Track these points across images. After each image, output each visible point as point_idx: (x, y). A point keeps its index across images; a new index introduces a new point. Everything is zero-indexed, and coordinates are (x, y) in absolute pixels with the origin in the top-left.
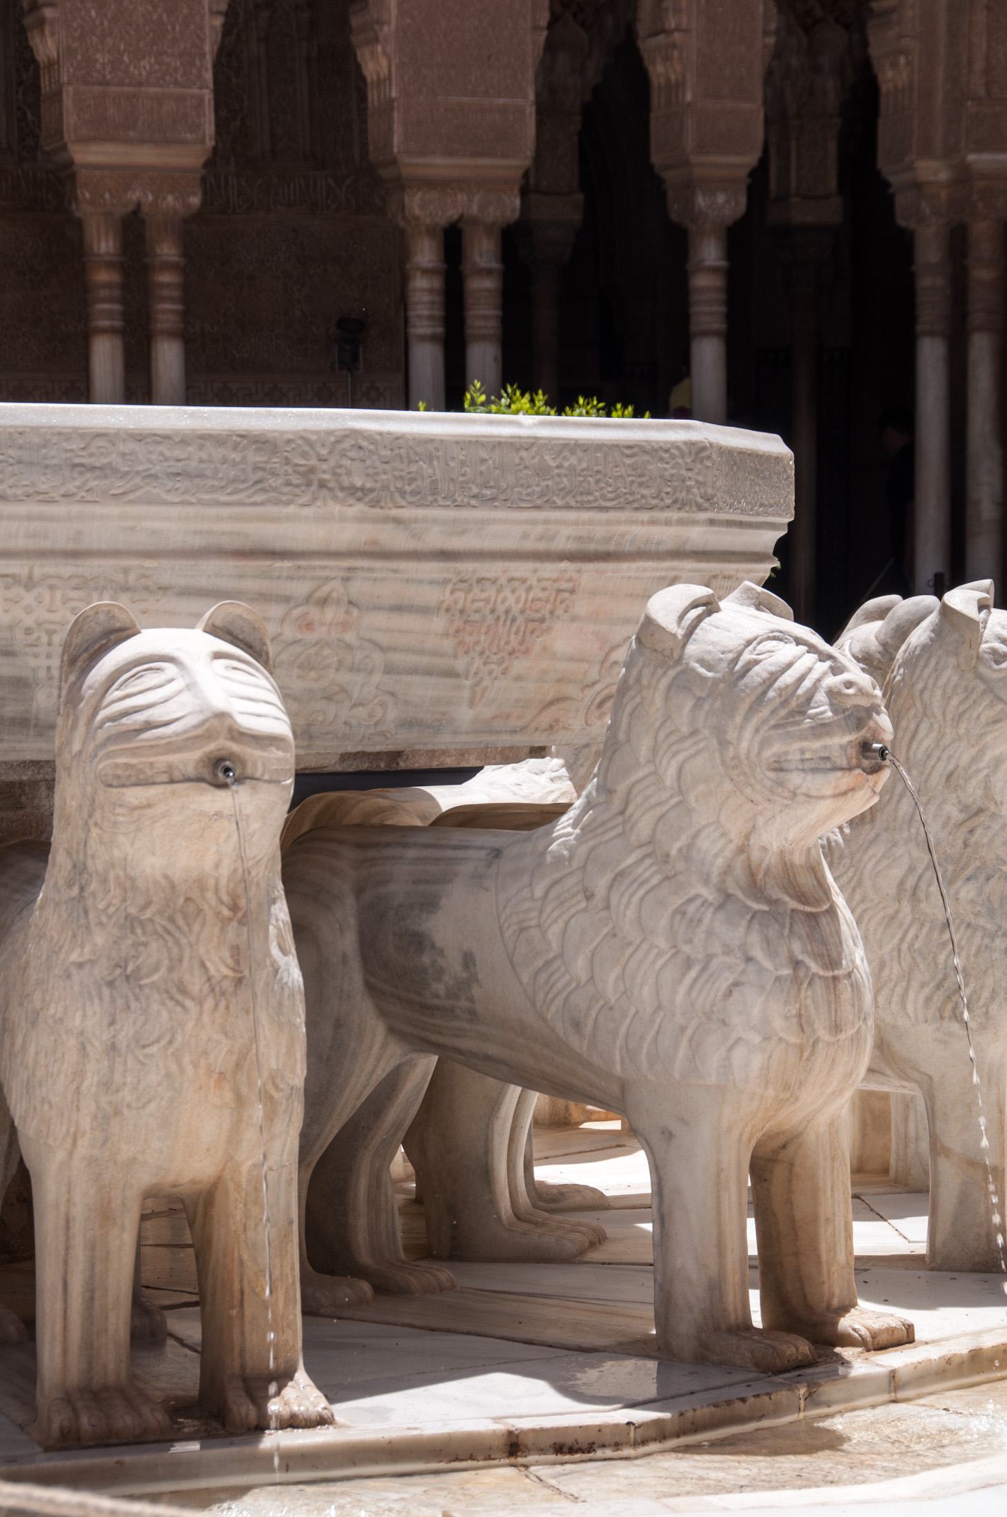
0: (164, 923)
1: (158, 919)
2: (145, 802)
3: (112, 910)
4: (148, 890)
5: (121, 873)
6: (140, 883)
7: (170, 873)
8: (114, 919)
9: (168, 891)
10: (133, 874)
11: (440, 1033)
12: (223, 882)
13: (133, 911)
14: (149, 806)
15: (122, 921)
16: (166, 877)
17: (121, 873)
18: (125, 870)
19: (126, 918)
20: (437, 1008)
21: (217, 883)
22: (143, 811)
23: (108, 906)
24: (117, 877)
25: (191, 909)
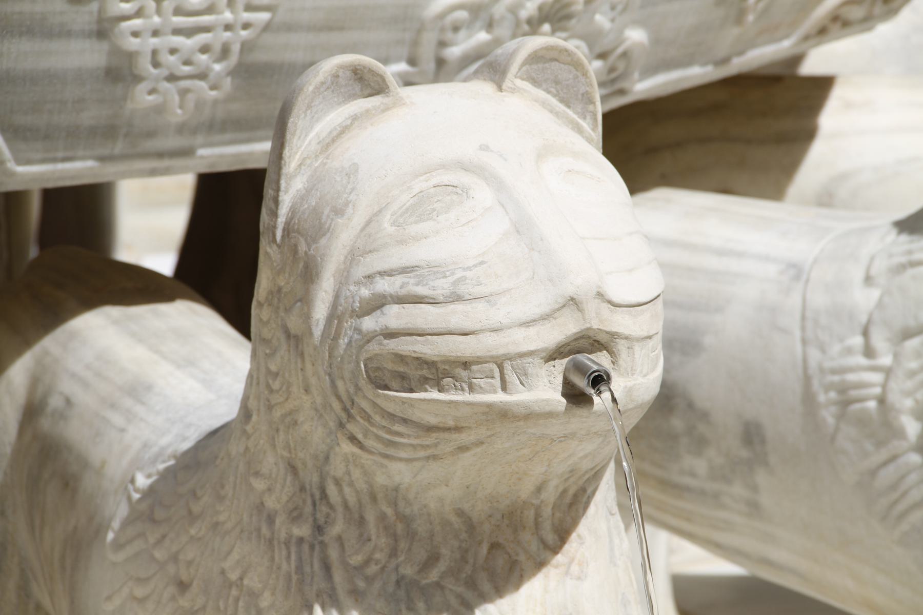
0: (460, 589)
1: (449, 583)
2: (451, 423)
4: (432, 536)
5: (389, 511)
6: (421, 527)
7: (466, 507)
8: (377, 585)
9: (464, 536)
10: (408, 511)
11: (688, 520)
12: (547, 511)
13: (408, 571)
14: (457, 429)
15: (391, 588)
16: (460, 513)
17: (389, 511)
18: (396, 505)
19: (398, 583)
20: (688, 489)
21: (538, 515)
22: (446, 435)
23: (367, 562)
24: (382, 517)
25: (500, 561)
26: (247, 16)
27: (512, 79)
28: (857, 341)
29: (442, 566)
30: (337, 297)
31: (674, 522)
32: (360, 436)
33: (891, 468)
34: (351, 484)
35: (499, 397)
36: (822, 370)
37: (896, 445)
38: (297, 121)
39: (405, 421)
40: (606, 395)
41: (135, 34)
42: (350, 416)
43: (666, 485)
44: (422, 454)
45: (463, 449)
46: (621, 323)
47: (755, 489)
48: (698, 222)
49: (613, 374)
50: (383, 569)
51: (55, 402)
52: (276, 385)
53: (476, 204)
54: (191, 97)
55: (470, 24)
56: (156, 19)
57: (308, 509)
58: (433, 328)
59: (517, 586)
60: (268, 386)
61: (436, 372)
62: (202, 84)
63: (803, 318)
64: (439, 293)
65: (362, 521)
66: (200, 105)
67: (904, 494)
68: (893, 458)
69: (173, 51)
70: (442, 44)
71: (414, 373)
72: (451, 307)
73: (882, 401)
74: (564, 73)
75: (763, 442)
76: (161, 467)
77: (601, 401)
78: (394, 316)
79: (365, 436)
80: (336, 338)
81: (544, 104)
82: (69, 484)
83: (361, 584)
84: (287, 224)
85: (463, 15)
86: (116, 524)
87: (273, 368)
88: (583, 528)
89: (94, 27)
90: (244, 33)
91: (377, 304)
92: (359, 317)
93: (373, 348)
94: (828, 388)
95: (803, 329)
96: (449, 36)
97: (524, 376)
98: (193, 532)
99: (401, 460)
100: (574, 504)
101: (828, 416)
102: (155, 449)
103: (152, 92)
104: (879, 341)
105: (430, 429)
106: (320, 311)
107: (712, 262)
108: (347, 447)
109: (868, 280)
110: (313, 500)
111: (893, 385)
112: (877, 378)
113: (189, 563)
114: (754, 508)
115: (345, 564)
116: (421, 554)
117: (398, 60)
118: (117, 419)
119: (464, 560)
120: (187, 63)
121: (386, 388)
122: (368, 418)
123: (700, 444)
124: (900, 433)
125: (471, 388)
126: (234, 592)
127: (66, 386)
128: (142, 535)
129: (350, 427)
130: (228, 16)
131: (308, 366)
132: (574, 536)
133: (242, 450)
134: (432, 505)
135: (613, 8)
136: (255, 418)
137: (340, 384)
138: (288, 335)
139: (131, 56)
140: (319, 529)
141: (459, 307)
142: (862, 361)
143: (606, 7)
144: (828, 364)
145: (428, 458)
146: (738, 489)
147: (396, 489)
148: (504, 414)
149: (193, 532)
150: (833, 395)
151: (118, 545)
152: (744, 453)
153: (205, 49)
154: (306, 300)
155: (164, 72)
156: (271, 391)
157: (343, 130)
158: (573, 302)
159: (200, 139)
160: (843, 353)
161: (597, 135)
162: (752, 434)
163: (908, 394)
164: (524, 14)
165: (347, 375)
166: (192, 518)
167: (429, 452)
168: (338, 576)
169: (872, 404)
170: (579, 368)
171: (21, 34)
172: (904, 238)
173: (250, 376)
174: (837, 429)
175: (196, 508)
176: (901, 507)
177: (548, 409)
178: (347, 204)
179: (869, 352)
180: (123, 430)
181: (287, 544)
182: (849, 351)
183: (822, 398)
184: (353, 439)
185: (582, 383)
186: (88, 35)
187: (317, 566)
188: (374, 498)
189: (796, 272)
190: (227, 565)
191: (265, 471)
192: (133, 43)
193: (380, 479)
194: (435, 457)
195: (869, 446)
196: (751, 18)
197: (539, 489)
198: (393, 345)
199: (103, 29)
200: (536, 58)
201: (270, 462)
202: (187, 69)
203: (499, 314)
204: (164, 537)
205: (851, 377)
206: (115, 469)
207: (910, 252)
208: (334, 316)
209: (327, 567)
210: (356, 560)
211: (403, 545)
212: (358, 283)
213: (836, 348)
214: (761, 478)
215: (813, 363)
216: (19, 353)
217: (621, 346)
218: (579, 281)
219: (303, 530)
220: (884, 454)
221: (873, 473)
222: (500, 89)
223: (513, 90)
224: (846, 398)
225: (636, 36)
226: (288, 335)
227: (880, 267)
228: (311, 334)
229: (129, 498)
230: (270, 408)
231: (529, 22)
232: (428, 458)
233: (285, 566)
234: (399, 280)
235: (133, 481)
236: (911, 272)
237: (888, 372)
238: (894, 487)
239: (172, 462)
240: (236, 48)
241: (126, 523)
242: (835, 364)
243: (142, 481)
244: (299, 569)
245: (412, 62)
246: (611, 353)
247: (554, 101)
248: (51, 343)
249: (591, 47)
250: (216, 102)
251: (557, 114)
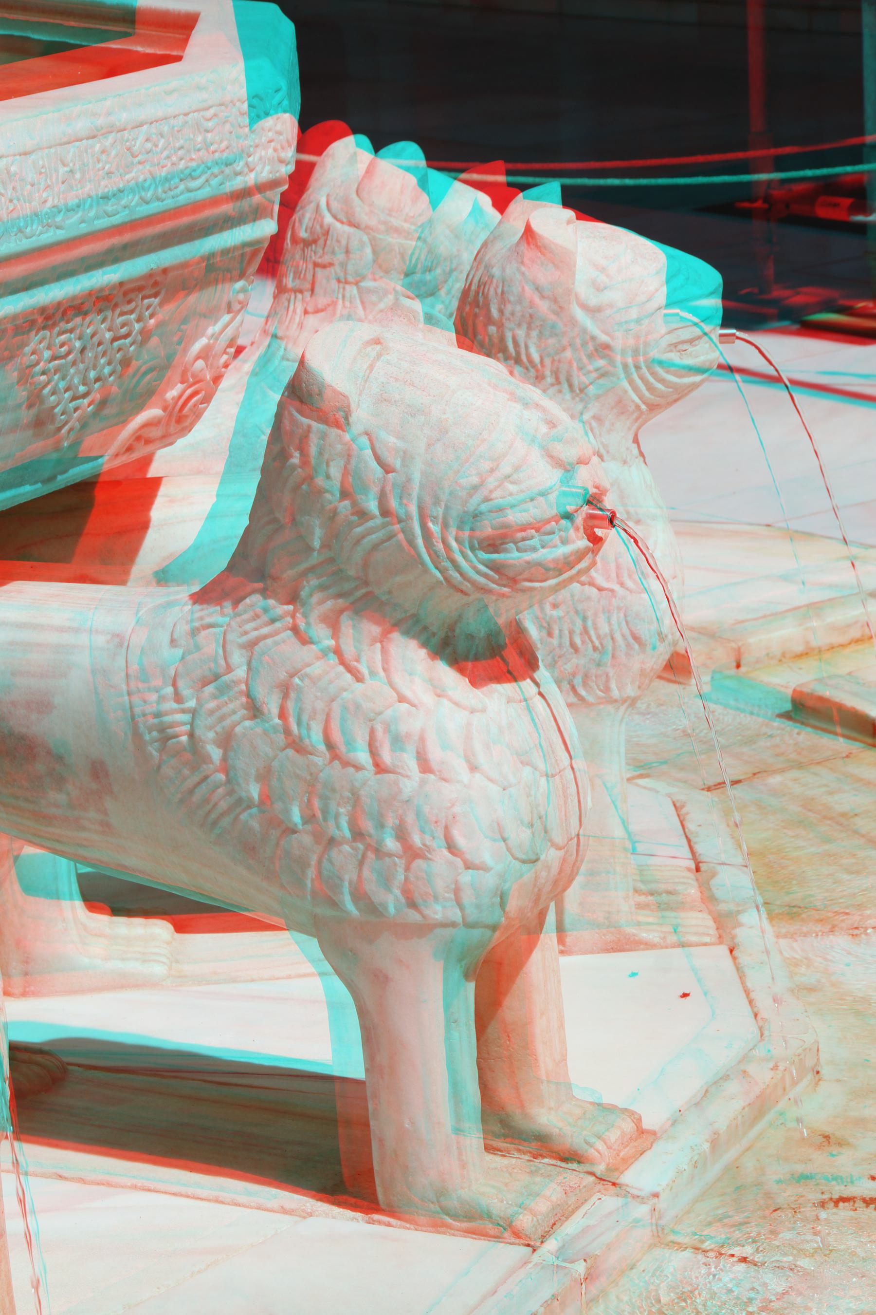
28: (170, 690)
31: (48, 844)
33: (204, 786)
36: (144, 715)
37: (206, 768)
47: (105, 812)
63: (127, 675)
67: (216, 804)
68: (206, 778)
73: (191, 735)
75: (107, 775)
95: (128, 685)
101: (153, 750)
107: (53, 638)
109: (173, 642)
111: (198, 722)
112: (187, 717)
114: (106, 827)
123: (60, 782)
124: (207, 759)
142: (175, 706)
144: (149, 710)
146: (92, 814)
150: (155, 734)
152: (94, 786)
160: (157, 700)
162: (98, 770)
163: (210, 728)
169: (184, 739)
172: (197, 607)
174: (161, 760)
176: (213, 816)
179: (178, 698)
183: (147, 737)
189: (120, 641)
195: (186, 772)
205: (167, 719)
207: (201, 618)
213: (154, 697)
214: (109, 803)
215: (137, 710)
220: (196, 778)
221: (191, 792)
224: (165, 736)
227: (183, 628)
236: (204, 633)
237: (194, 712)
238: (206, 801)
242: (154, 709)
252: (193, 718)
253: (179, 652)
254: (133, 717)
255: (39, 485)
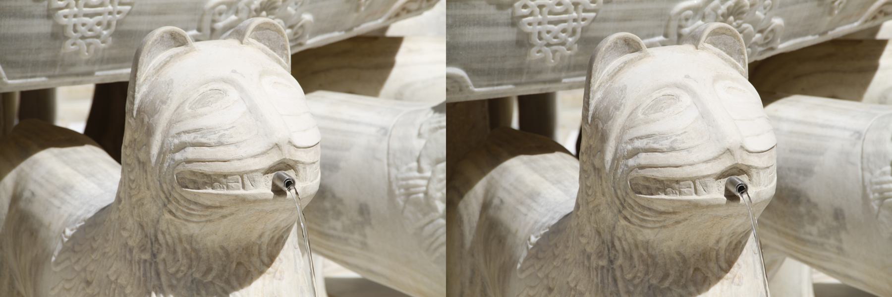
0: (222, 285)
1: (217, 282)
2: (218, 204)
3: (180, 275)
4: (209, 259)
6: (204, 255)
7: (225, 245)
8: (182, 282)
10: (197, 247)
12: (264, 247)
14: (221, 207)
15: (189, 284)
16: (222, 248)
19: (192, 281)
20: (332, 236)
21: (260, 249)
22: (216, 210)
23: (177, 272)
25: (242, 271)
26: (119, 8)
27: (247, 38)
28: (414, 164)
29: (214, 274)
30: (163, 143)
32: (174, 211)
33: (431, 226)
34: (170, 234)
35: (241, 192)
37: (433, 215)
38: (144, 59)
39: (196, 203)
40: (293, 191)
41: (65, 17)
42: (169, 201)
43: (322, 234)
44: (204, 219)
45: (224, 217)
46: (300, 156)
47: (365, 236)
48: (337, 107)
49: (296, 181)
50: (185, 275)
51: (27, 194)
52: (133, 186)
53: (230, 99)
54: (92, 47)
55: (227, 12)
56: (76, 9)
57: (149, 246)
58: (209, 158)
59: (250, 283)
60: (130, 187)
61: (211, 180)
62: (98, 41)
63: (388, 154)
64: (212, 142)
65: (175, 252)
66: (96, 50)
67: (438, 238)
68: (432, 221)
69: (84, 25)
70: (214, 21)
71: (200, 180)
72: (218, 148)
73: (426, 193)
74: (273, 35)
76: (78, 225)
77: (290, 194)
78: (191, 153)
79: (177, 210)
80: (162, 163)
81: (263, 50)
82: (33, 233)
83: (175, 282)
84: (139, 108)
85: (223, 7)
86: (56, 253)
87: (132, 178)
88: (282, 255)
89: (46, 13)
90: (118, 16)
91: (182, 147)
92: (174, 153)
93: (180, 168)
94: (400, 187)
95: (388, 159)
96: (217, 17)
97: (253, 182)
98: (93, 257)
99: (193, 222)
100: (277, 243)
102: (75, 217)
103: (73, 44)
104: (425, 165)
105: (208, 207)
106: (155, 150)
108: (168, 216)
109: (420, 135)
110: (152, 242)
111: (431, 186)
112: (423, 182)
113: (92, 272)
115: (167, 273)
116: (203, 268)
117: (192, 29)
118: (56, 202)
119: (224, 270)
120: (90, 30)
121: (187, 187)
122: (178, 202)
123: (338, 215)
125: (228, 188)
126: (113, 286)
127: (32, 186)
128: (68, 258)
129: (169, 206)
130: (110, 8)
131: (149, 177)
132: (277, 259)
133: (117, 217)
134: (209, 244)
135: (296, 4)
136: (123, 202)
137: (164, 186)
138: (139, 162)
139: (63, 27)
140: (154, 255)
141: (222, 148)
142: (417, 174)
143: (293, 4)
144: (400, 176)
145: (207, 221)
146: (356, 236)
147: (192, 236)
148: (243, 200)
149: (93, 257)
150: (402, 191)
151: (57, 263)
153: (99, 24)
154: (148, 145)
155: (79, 35)
156: (131, 189)
157: (166, 63)
158: (277, 146)
159: (96, 67)
161: (289, 65)
162: (363, 210)
164: (253, 7)
165: (168, 181)
166: (93, 250)
167: (208, 218)
168: (163, 278)
169: (421, 195)
170: (280, 178)
171: (10, 17)
173: (121, 182)
174: (404, 207)
175: (95, 246)
176: (435, 245)
177: (265, 197)
178: (168, 98)
179: (420, 170)
180: (59, 208)
181: (139, 263)
182: (410, 169)
184: (170, 212)
185: (281, 185)
186: (43, 17)
187: (153, 273)
188: (181, 241)
190: (109, 273)
191: (128, 227)
192: (64, 21)
193: (184, 231)
194: (210, 221)
195: (420, 216)
196: (363, 9)
197: (260, 236)
198: (190, 167)
199: (50, 14)
200: (259, 28)
201: (130, 223)
202: (90, 33)
203: (241, 152)
204: (79, 259)
205: (411, 182)
206: (56, 226)
208: (161, 152)
209: (158, 274)
210: (172, 270)
211: (195, 263)
212: (173, 137)
213: (404, 168)
214: (368, 230)
216: (9, 170)
217: (300, 167)
218: (280, 136)
219: (146, 256)
220: (427, 219)
221: (422, 228)
222: (242, 43)
223: (248, 44)
224: (409, 192)
225: (307, 17)
226: (139, 162)
227: (425, 129)
228: (150, 161)
229: (62, 241)
230: (130, 197)
231: (256, 10)
232: (207, 221)
233: (138, 274)
234: (193, 135)
235: (64, 232)
237: (429, 180)
238: (432, 235)
239: (83, 223)
240: (114, 23)
241: (61, 253)
242: (404, 176)
243: (69, 232)
244: (145, 274)
245: (199, 30)
246: (295, 170)
247: (268, 49)
248: (24, 166)
249: (285, 22)
250: (104, 49)
251: (269, 55)
252: (428, 183)
253: (423, 142)
254: (389, 178)
255: (817, 37)
